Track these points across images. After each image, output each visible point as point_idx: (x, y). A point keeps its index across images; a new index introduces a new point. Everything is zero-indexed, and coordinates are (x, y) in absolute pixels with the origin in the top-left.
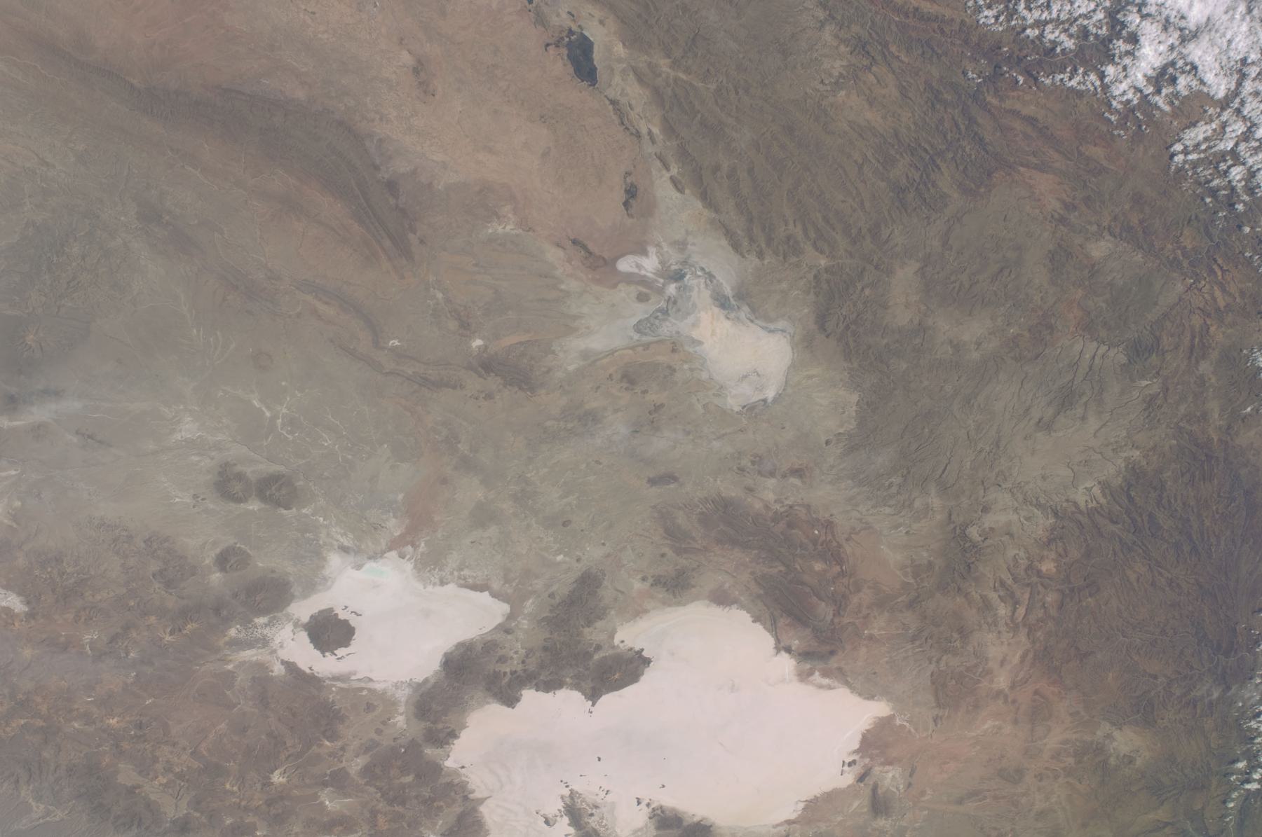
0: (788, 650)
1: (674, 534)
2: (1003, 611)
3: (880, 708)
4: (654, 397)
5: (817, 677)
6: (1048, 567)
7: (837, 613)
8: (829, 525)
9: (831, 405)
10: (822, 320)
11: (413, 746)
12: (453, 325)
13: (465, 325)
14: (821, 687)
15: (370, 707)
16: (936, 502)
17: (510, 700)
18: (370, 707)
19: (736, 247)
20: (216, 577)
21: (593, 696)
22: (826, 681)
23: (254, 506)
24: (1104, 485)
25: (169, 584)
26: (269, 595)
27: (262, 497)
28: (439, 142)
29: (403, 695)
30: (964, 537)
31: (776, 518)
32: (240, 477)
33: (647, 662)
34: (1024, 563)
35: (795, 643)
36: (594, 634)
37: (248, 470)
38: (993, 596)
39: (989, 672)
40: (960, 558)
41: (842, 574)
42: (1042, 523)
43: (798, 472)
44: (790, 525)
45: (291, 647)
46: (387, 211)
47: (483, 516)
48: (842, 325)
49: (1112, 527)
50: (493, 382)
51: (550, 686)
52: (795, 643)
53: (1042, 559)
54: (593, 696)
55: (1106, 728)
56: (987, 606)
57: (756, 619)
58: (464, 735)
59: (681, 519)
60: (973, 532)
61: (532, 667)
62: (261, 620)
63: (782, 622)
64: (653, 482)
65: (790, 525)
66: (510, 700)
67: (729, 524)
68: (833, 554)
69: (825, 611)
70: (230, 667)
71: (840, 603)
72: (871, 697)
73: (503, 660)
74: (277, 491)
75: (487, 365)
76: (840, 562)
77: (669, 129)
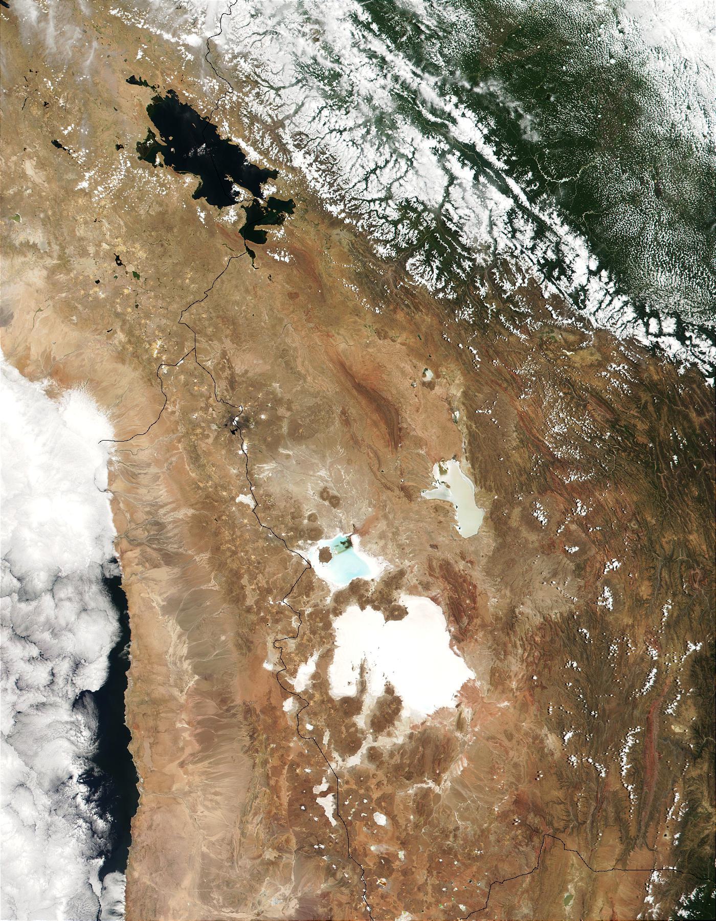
0: (450, 631)
1: (431, 567)
2: (520, 651)
3: (472, 675)
4: (441, 518)
5: (455, 648)
6: (538, 639)
7: (468, 624)
8: (475, 587)
9: (489, 543)
10: (492, 514)
11: (328, 612)
12: (399, 473)
13: (402, 474)
14: (455, 653)
15: (323, 590)
16: (508, 593)
17: (363, 608)
18: (323, 590)
19: (476, 482)
20: (306, 521)
21: (387, 619)
22: (457, 651)
23: (327, 503)
24: (561, 614)
25: (293, 518)
26: (315, 534)
27: (330, 502)
28: (415, 422)
29: (333, 590)
30: (514, 612)
31: (461, 576)
32: (328, 492)
33: (407, 613)
34: (530, 633)
35: (453, 629)
36: (395, 594)
37: (331, 492)
38: (518, 643)
39: (510, 677)
40: (510, 621)
41: (474, 608)
42: (538, 620)
43: (472, 562)
44: (464, 581)
45: (311, 554)
46: (396, 434)
47: (382, 536)
48: (496, 520)
49: (561, 634)
50: (402, 494)
51: (376, 608)
52: (453, 629)
53: (536, 635)
54: (387, 619)
55: (545, 730)
56: (515, 646)
57: (444, 613)
58: (344, 614)
59: (434, 564)
60: (517, 611)
61: (374, 598)
62: (309, 542)
63: (452, 618)
64: (432, 546)
65: (464, 581)
66: (363, 608)
67: (447, 572)
68: (474, 601)
69: (465, 620)
70: (293, 554)
71: (471, 618)
72: (469, 667)
73: (367, 590)
74: (335, 502)
75: (403, 488)
76: (475, 603)
77: (470, 443)
